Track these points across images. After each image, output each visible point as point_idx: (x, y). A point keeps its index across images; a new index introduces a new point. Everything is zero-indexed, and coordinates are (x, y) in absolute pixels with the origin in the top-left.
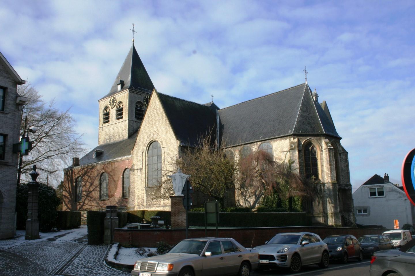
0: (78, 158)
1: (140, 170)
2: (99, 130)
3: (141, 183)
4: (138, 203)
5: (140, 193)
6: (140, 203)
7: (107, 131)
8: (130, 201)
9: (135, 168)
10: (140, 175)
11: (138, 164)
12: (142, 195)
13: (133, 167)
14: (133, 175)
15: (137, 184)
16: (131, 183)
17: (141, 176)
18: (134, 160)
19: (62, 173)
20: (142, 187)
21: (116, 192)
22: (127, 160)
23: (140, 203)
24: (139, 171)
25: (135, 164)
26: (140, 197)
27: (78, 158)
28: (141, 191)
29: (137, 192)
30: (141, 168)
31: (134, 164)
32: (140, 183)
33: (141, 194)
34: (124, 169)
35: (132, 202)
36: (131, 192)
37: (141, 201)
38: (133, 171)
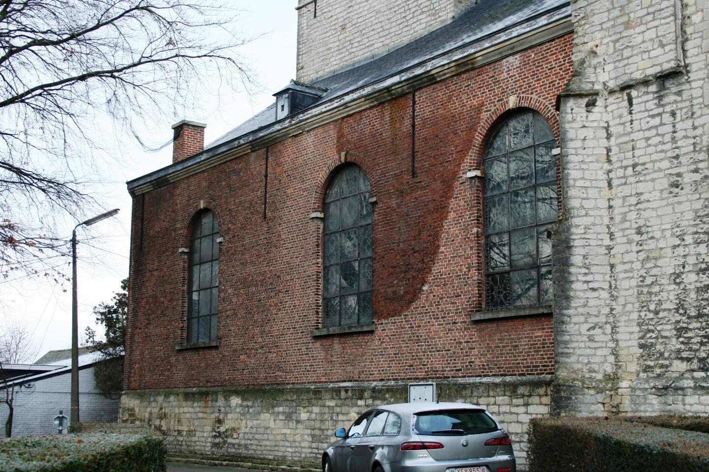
0: (199, 129)
1: (662, 88)
2: (300, 16)
3: (676, 185)
4: (642, 346)
5: (668, 265)
6: (674, 344)
7: (339, 10)
8: (571, 328)
9: (601, 76)
10: (657, 121)
11: (639, 39)
12: (690, 279)
13: (589, 71)
14: (589, 133)
15: (633, 200)
16: (572, 192)
17: (669, 128)
18: (596, 19)
19: (126, 204)
20: (690, 215)
21: (430, 278)
22: (514, 61)
23: (674, 344)
24: (644, 99)
25: (598, 50)
26: (669, 295)
27: (199, 129)
28: (680, 251)
29: (633, 256)
30: (666, 61)
31: (593, 53)
32: (665, 183)
33: (676, 278)
34: (487, 117)
35: (591, 339)
36: (576, 260)
37: (680, 331)
38: (591, 104)
